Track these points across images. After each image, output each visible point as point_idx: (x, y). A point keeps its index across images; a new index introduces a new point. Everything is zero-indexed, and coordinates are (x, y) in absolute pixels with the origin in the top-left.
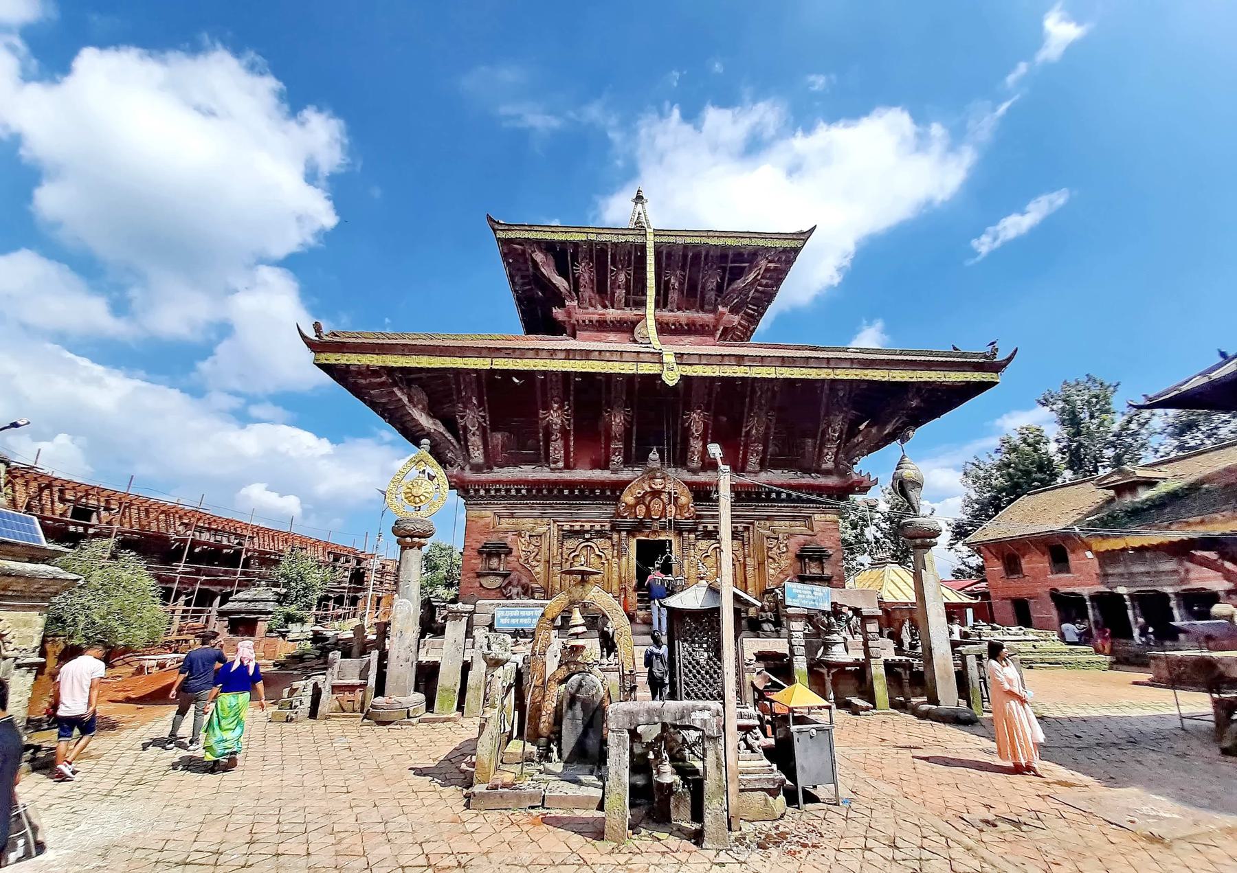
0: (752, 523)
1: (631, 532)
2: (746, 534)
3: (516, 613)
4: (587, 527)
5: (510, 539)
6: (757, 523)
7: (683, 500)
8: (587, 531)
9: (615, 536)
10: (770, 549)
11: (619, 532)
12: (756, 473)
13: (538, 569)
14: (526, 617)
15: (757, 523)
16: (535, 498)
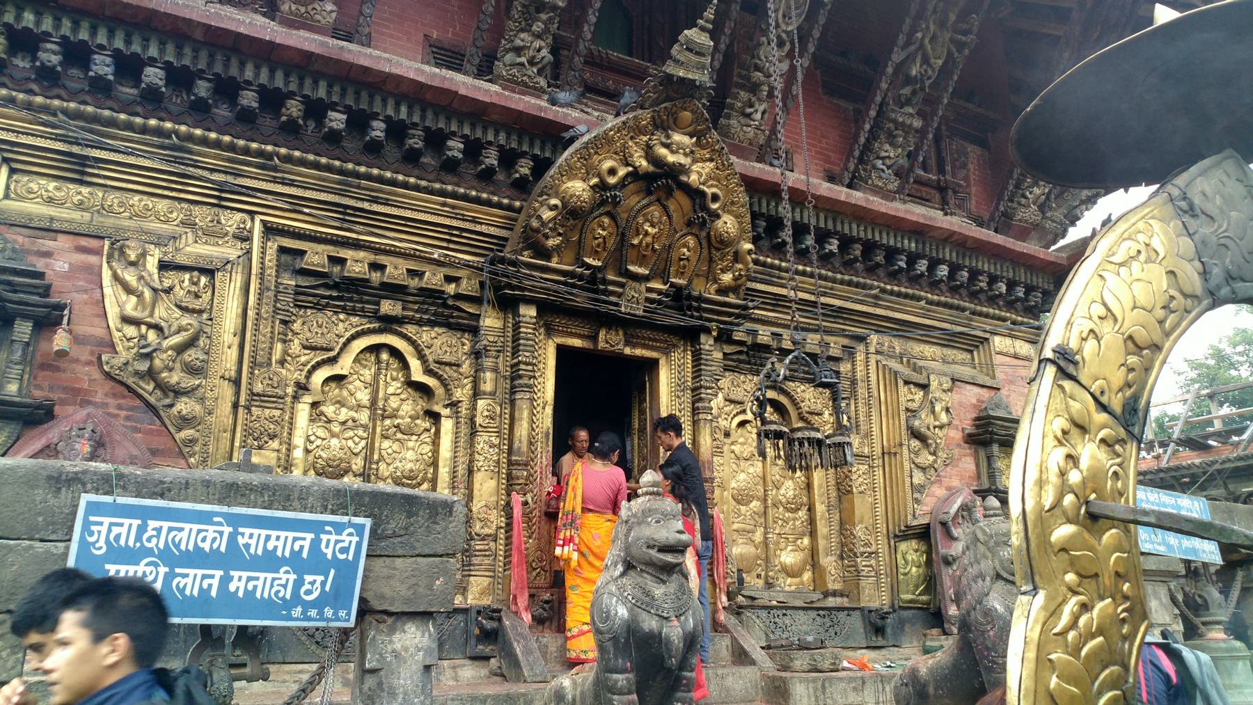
0: (861, 339)
1: (553, 312)
2: (845, 368)
3: (213, 537)
4: (396, 270)
5: (60, 263)
6: (874, 338)
7: (727, 224)
8: (394, 290)
9: (491, 321)
10: (912, 412)
11: (507, 305)
12: (887, 195)
13: (184, 406)
14: (269, 562)
15: (874, 338)
16: (199, 111)
